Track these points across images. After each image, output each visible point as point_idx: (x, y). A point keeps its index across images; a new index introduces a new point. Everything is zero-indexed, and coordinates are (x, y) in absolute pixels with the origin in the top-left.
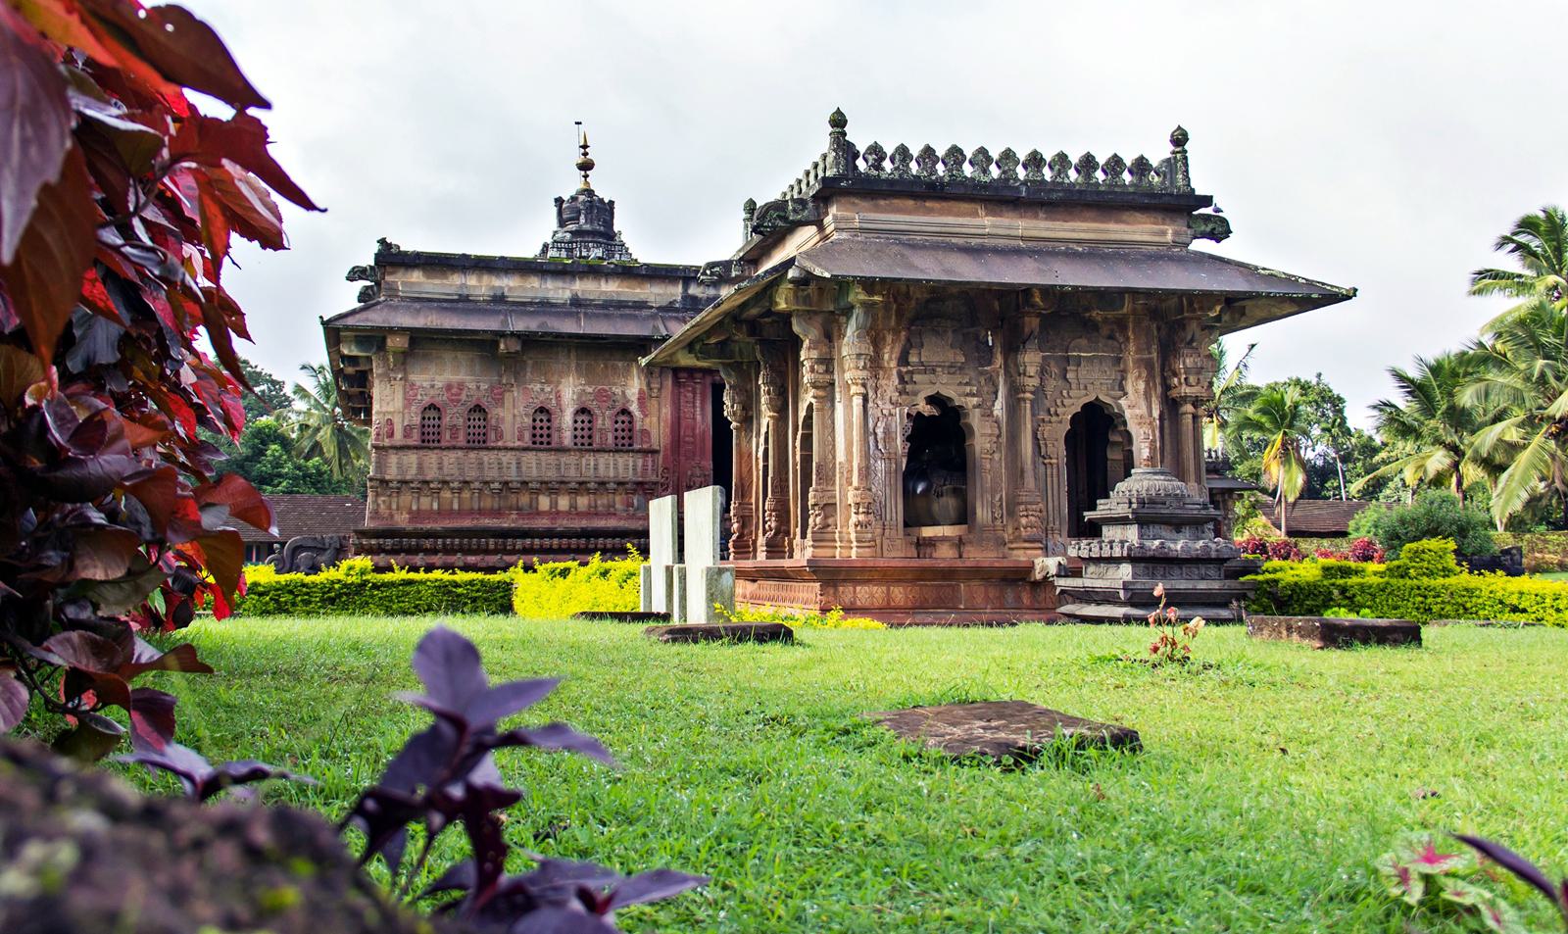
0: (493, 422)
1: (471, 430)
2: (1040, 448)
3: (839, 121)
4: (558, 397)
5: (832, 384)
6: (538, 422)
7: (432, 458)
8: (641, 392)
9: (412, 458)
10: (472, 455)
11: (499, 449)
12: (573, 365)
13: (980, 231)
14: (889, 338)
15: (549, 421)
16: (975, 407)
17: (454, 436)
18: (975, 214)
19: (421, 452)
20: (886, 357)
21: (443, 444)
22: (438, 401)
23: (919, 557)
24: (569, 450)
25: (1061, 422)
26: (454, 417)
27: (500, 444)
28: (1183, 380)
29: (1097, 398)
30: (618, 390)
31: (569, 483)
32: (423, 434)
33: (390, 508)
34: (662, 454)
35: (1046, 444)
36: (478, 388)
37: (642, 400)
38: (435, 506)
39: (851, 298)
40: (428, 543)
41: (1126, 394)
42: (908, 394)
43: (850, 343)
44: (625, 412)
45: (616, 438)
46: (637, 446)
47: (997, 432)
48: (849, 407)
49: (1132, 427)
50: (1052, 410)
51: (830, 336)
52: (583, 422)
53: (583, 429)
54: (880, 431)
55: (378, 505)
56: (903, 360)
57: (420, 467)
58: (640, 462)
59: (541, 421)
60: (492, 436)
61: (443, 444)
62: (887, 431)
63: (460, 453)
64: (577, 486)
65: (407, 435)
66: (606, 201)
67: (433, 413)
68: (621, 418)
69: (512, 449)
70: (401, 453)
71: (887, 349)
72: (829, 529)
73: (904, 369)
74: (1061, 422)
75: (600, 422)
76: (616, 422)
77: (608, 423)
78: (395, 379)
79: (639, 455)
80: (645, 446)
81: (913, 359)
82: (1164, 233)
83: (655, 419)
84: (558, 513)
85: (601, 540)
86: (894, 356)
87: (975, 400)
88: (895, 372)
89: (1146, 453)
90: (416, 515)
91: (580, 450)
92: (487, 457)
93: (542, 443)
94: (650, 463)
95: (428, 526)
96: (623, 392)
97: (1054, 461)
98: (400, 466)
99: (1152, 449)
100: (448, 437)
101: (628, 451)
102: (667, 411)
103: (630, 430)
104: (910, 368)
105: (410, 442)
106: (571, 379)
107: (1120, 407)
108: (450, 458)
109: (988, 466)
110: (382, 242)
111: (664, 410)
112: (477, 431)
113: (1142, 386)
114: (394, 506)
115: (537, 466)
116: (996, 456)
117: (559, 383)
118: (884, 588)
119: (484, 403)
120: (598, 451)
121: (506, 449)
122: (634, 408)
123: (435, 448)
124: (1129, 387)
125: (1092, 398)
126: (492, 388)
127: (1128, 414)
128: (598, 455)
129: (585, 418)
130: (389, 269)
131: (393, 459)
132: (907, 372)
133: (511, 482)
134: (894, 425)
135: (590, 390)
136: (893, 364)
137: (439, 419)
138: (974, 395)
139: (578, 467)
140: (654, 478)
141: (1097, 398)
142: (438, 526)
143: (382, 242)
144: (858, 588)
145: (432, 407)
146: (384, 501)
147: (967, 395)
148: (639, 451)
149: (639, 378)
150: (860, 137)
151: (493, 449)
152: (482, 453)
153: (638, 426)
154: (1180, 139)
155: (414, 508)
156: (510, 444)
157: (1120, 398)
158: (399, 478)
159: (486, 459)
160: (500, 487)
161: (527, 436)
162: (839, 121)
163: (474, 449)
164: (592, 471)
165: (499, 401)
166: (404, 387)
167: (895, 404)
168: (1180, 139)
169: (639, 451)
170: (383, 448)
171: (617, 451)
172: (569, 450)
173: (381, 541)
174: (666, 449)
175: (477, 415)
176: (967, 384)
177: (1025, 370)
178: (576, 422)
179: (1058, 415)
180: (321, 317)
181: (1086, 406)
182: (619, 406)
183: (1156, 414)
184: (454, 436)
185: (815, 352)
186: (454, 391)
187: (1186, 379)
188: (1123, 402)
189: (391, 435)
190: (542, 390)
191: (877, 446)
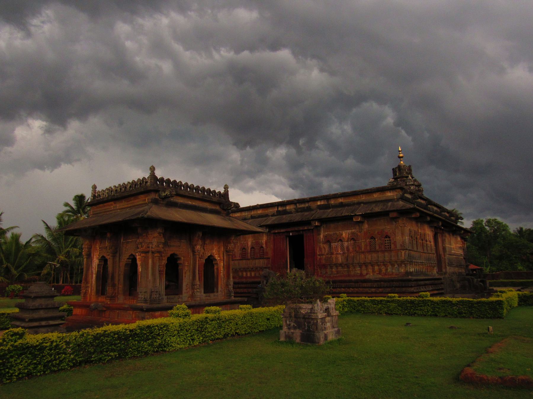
4: (248, 245)
8: (266, 241)
24: (249, 259)
27: (235, 259)
30: (260, 241)
37: (266, 243)
44: (262, 247)
82: (145, 200)
83: (269, 248)
111: (271, 246)
115: (243, 264)
120: (255, 259)
122: (264, 246)
128: (256, 260)
148: (265, 258)
149: (265, 237)
153: (265, 251)
169: (265, 258)
171: (260, 259)
172: (249, 259)
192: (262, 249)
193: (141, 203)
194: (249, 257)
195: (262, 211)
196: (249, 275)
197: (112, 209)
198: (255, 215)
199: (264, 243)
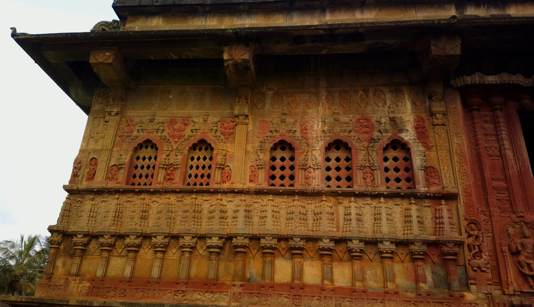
0: (219, 159)
1: (193, 172)
6: (278, 160)
11: (225, 192)
15: (292, 159)
17: (169, 178)
22: (155, 137)
27: (226, 186)
34: (462, 199)
52: (338, 160)
53: (338, 169)
57: (118, 216)
59: (283, 159)
60: (217, 176)
65: (111, 174)
67: (147, 152)
70: (99, 199)
76: (386, 159)
78: (110, 113)
80: (434, 189)
84: (303, 287)
91: (335, 194)
103: (407, 170)
105: (111, 185)
111: (455, 141)
112: (200, 172)
117: (305, 113)
119: (210, 138)
126: (222, 121)
129: (342, 154)
133: (236, 236)
137: (156, 158)
140: (455, 236)
145: (148, 143)
151: (216, 192)
155: (99, 273)
156: (238, 186)
159: (206, 206)
160: (220, 243)
163: (191, 192)
164: (354, 222)
165: (230, 135)
174: (468, 194)
178: (328, 160)
182: (386, 138)
184: (169, 178)
189: (92, 177)
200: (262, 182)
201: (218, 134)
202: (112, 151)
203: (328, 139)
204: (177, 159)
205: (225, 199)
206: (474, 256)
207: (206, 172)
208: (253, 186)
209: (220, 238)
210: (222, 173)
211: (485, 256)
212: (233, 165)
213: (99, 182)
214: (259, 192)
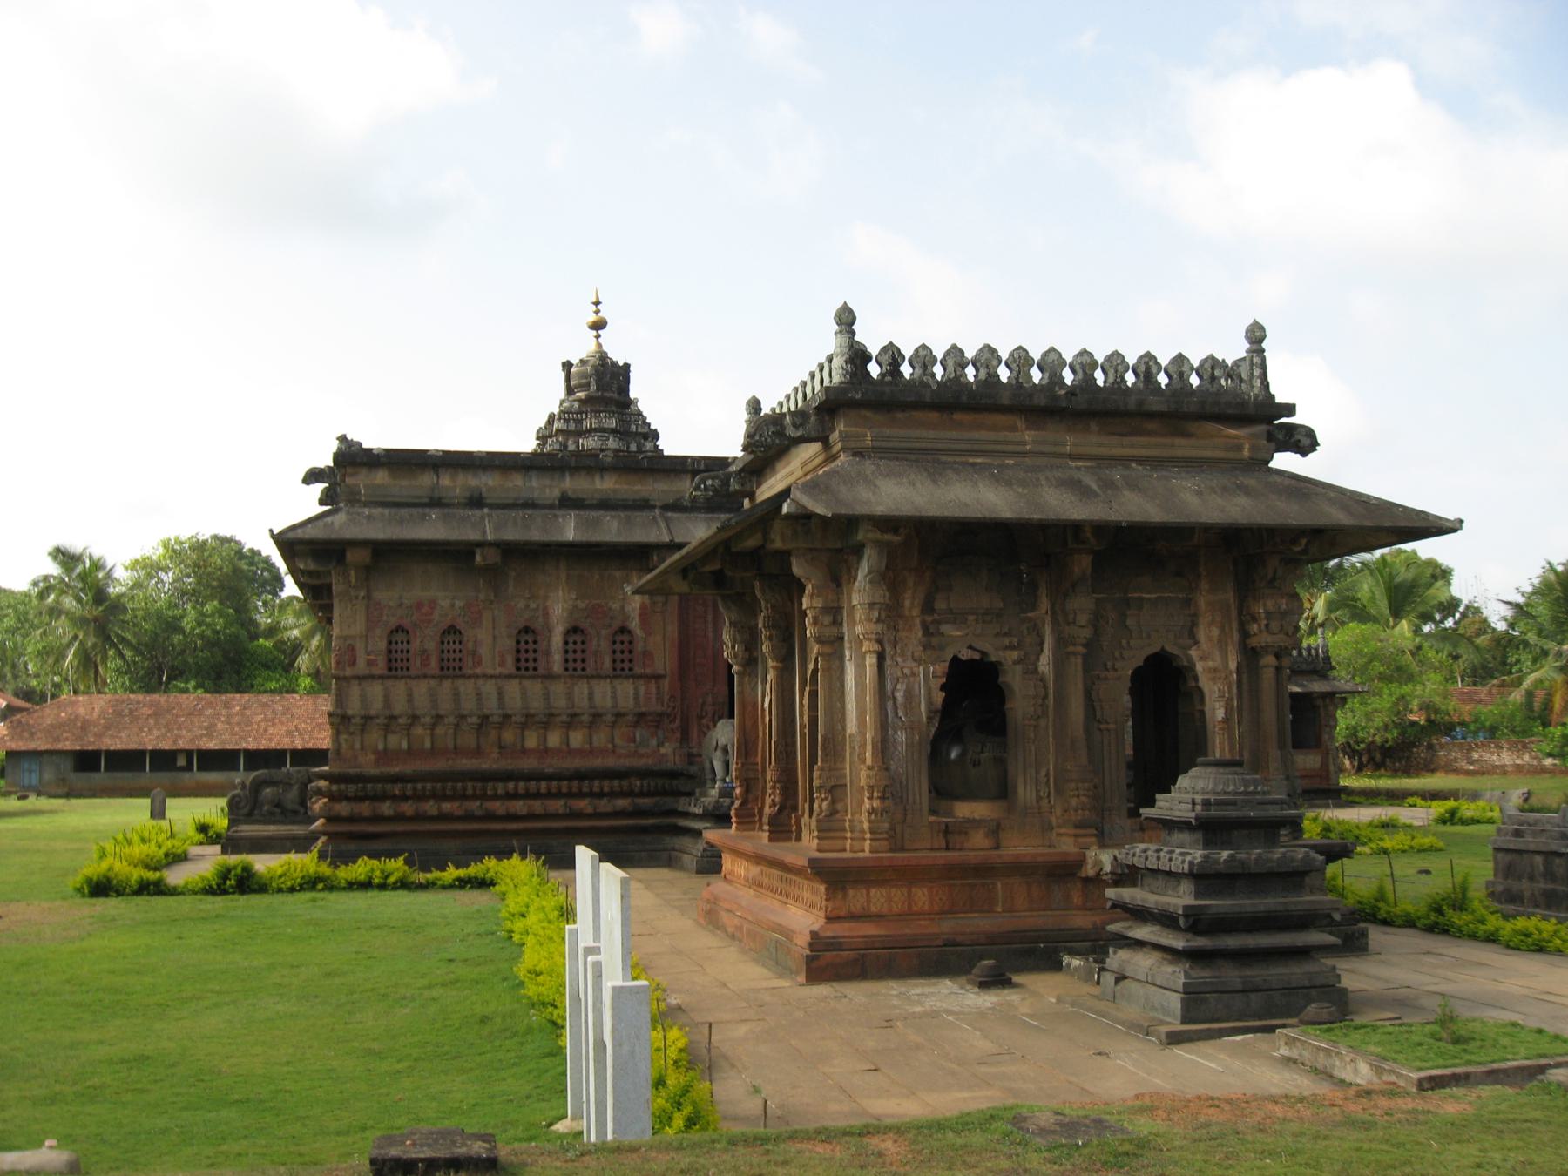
0: (470, 645)
2: (1094, 710)
3: (846, 319)
4: (546, 615)
5: (842, 638)
7: (399, 689)
9: (376, 690)
10: (447, 684)
11: (477, 676)
12: (563, 575)
13: (1019, 449)
14: (910, 582)
15: (535, 642)
16: (1015, 663)
17: (425, 662)
18: (1013, 429)
19: (389, 683)
20: (907, 603)
21: (413, 672)
22: (406, 623)
23: (947, 849)
24: (559, 677)
25: (1119, 678)
26: (426, 641)
27: (478, 671)
28: (1263, 627)
29: (1163, 649)
30: (616, 606)
31: (559, 715)
32: (390, 661)
33: (352, 747)
35: (1102, 708)
36: (453, 606)
38: (405, 745)
39: (860, 536)
40: (397, 789)
41: (1196, 643)
42: (933, 648)
43: (861, 592)
44: (623, 630)
45: (614, 661)
46: (638, 670)
47: (1042, 692)
48: (860, 668)
49: (1205, 683)
50: (1109, 664)
51: (837, 578)
52: (575, 643)
53: (575, 652)
54: (899, 695)
55: (339, 744)
56: (928, 608)
58: (642, 689)
61: (413, 672)
62: (909, 694)
63: (433, 683)
64: (568, 719)
66: (621, 364)
67: (400, 637)
68: (619, 638)
69: (492, 677)
71: (908, 594)
72: (838, 816)
73: (929, 619)
74: (1119, 678)
75: (595, 642)
76: (614, 643)
77: (605, 645)
78: (357, 598)
79: (641, 682)
80: (648, 671)
81: (940, 605)
84: (547, 750)
85: (597, 783)
86: (916, 603)
87: (1015, 654)
88: (918, 621)
89: (1220, 714)
90: (384, 756)
91: (572, 677)
92: (466, 687)
93: (527, 669)
94: (654, 690)
95: (395, 769)
96: (623, 608)
97: (1112, 726)
98: (364, 700)
99: (1228, 710)
100: (418, 663)
101: (627, 677)
102: (673, 629)
103: (630, 652)
104: (936, 616)
106: (561, 593)
107: (1190, 659)
108: (421, 689)
109: (1032, 735)
110: (343, 439)
113: (1215, 632)
114: (358, 746)
115: (519, 695)
116: (1042, 722)
117: (546, 598)
118: (905, 890)
119: (460, 625)
120: (592, 677)
121: (486, 676)
122: (635, 625)
123: (402, 677)
124: (1202, 634)
125: (1156, 648)
127: (1199, 667)
128: (594, 682)
129: (578, 638)
130: (349, 470)
131: (355, 691)
132: (933, 622)
133: (492, 715)
134: (916, 687)
135: (582, 605)
136: (916, 612)
137: (408, 642)
138: (1012, 647)
139: (569, 696)
140: (659, 709)
141: (1163, 649)
142: (408, 768)
143: (343, 439)
144: (873, 891)
145: (399, 629)
146: (346, 740)
147: (1006, 648)
148: (640, 677)
150: (872, 338)
151: (470, 677)
152: (460, 682)
153: (639, 647)
154: (1256, 335)
155: (381, 747)
156: (490, 671)
157: (1190, 648)
158: (363, 713)
159: (462, 689)
161: (510, 660)
162: (846, 319)
163: (447, 677)
166: (368, 607)
167: (918, 661)
168: (1256, 335)
169: (640, 677)
170: (345, 678)
171: (616, 677)
173: (343, 786)
175: (451, 638)
176: (1006, 635)
177: (1074, 619)
178: (566, 643)
179: (1116, 670)
180: (271, 531)
181: (1147, 659)
182: (616, 625)
183: (1233, 666)
185: (820, 600)
186: (425, 609)
187: (1267, 625)
188: (1193, 653)
189: (353, 663)
190: (527, 606)
191: (897, 714)
192: (626, 638)
193: (1209, 453)
194: (557, 667)
195: (616, 482)
196: (554, 739)
197: (1028, 447)
198: (584, 497)
199: (637, 612)
200: (510, 667)
201: (466, 619)
202: (367, 636)
203: (567, 625)
204: (431, 645)
205: (480, 682)
206: (670, 722)
207: (458, 655)
208: (505, 671)
209: (479, 717)
210: (473, 658)
211: (678, 722)
212: (484, 651)
213: (361, 667)
214: (509, 677)
